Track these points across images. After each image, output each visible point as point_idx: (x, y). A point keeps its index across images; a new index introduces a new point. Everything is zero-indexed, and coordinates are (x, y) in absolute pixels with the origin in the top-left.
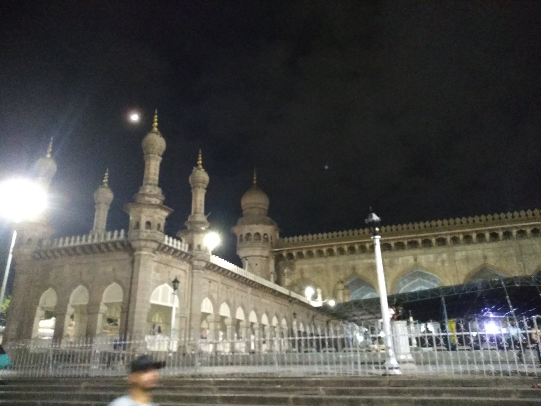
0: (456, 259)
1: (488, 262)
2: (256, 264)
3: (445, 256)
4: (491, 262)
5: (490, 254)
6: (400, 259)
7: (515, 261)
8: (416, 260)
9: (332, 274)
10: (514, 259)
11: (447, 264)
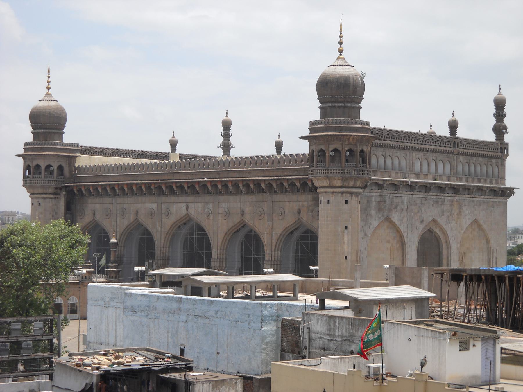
0: (220, 212)
1: (244, 219)
2: (40, 204)
3: (211, 206)
4: (248, 219)
5: (248, 209)
6: (175, 206)
7: (266, 220)
8: (187, 208)
9: (118, 219)
10: (266, 217)
11: (211, 218)
